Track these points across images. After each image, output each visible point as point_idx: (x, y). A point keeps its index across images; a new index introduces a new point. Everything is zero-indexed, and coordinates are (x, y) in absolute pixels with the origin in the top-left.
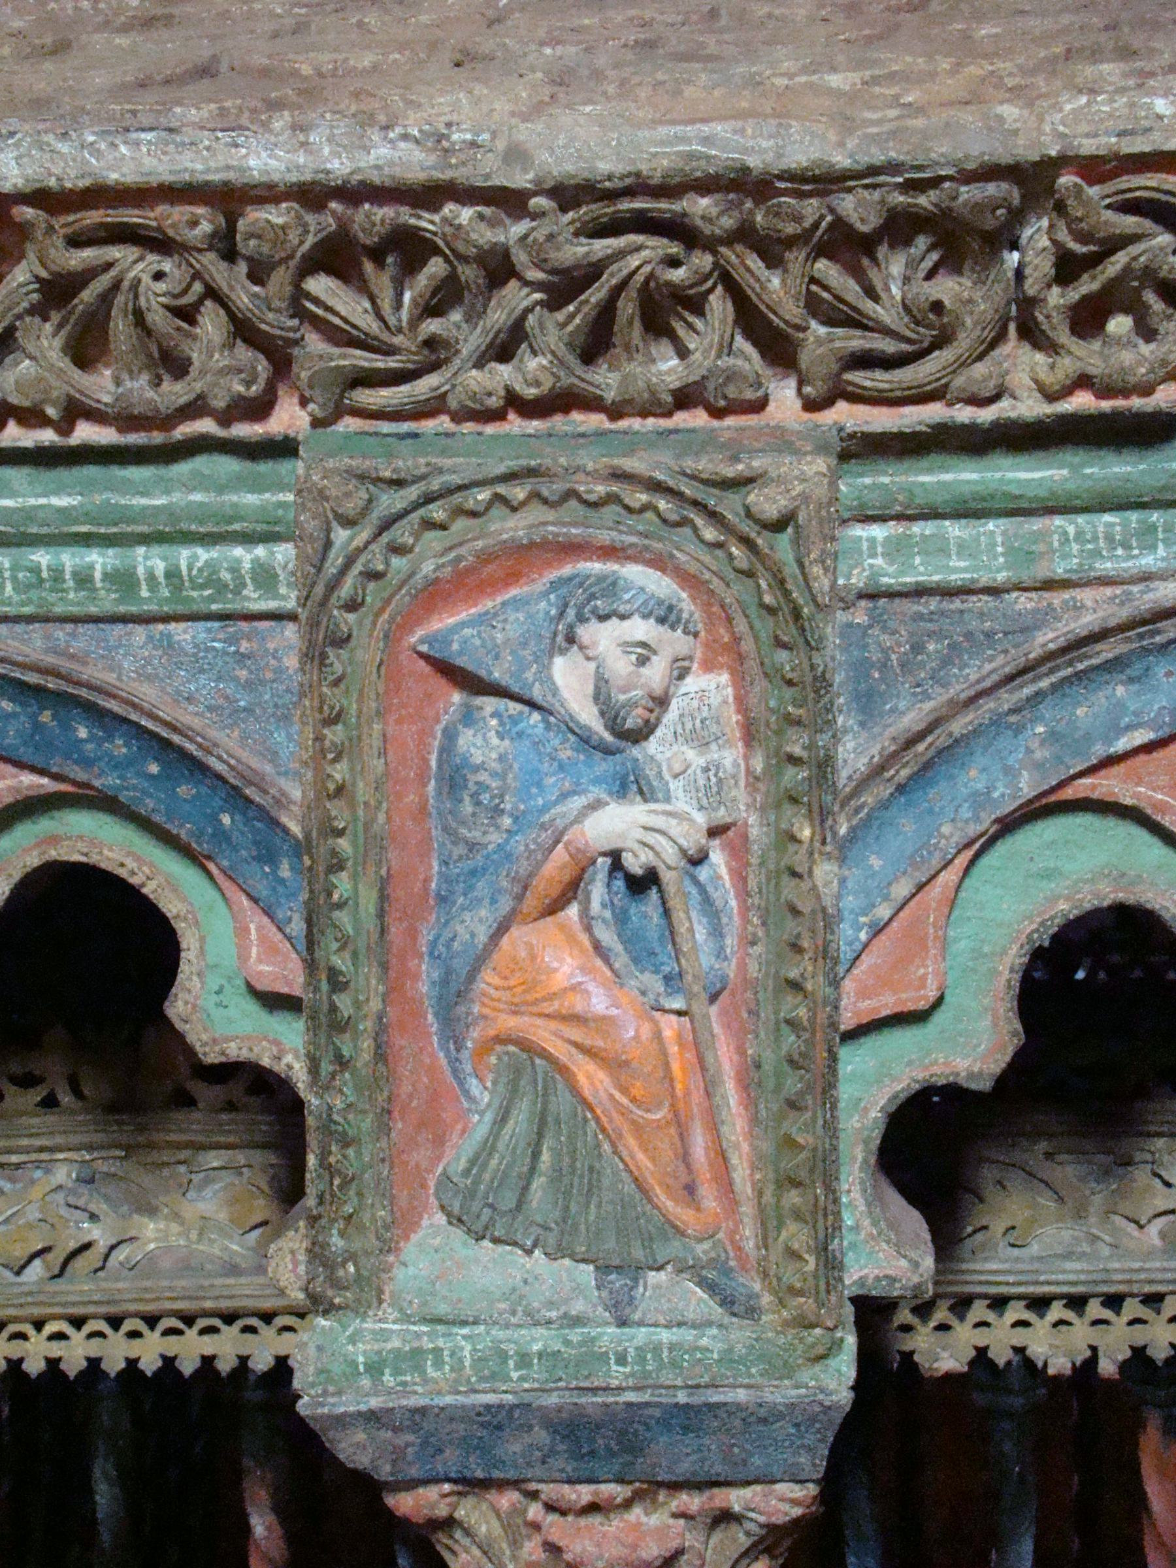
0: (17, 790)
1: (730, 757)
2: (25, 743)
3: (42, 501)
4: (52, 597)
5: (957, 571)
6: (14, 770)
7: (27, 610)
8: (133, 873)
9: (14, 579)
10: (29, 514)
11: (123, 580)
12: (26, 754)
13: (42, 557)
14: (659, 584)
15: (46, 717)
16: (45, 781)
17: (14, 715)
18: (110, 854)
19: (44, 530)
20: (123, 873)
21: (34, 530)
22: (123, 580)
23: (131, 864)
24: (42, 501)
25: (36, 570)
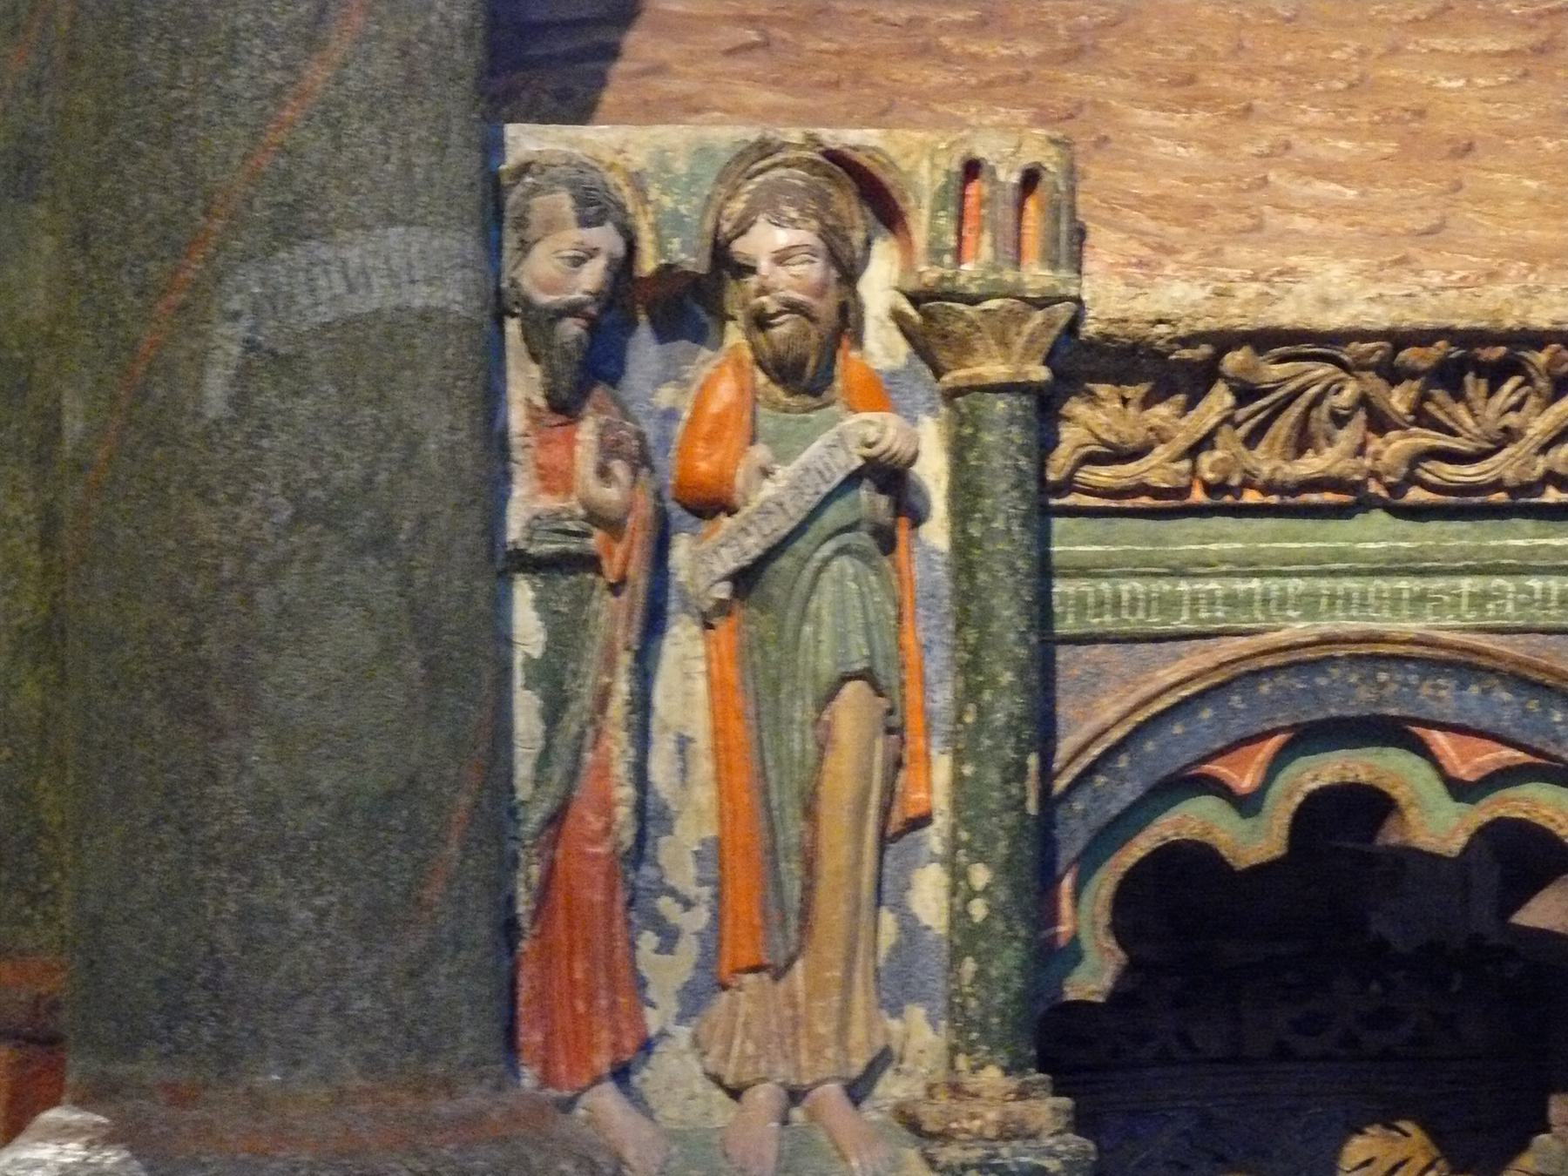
0: (1497, 761)
2: (1516, 726)
3: (1544, 541)
4: (1540, 613)
6: (1496, 746)
7: (1520, 623)
8: (1561, 827)
9: (1515, 600)
10: (1533, 550)
12: (1515, 733)
13: (1535, 583)
15: (1533, 705)
16: (1519, 754)
17: (1508, 704)
18: (1545, 812)
19: (1543, 563)
20: (1551, 826)
21: (1534, 563)
23: (1560, 819)
24: (1544, 541)
25: (1531, 592)
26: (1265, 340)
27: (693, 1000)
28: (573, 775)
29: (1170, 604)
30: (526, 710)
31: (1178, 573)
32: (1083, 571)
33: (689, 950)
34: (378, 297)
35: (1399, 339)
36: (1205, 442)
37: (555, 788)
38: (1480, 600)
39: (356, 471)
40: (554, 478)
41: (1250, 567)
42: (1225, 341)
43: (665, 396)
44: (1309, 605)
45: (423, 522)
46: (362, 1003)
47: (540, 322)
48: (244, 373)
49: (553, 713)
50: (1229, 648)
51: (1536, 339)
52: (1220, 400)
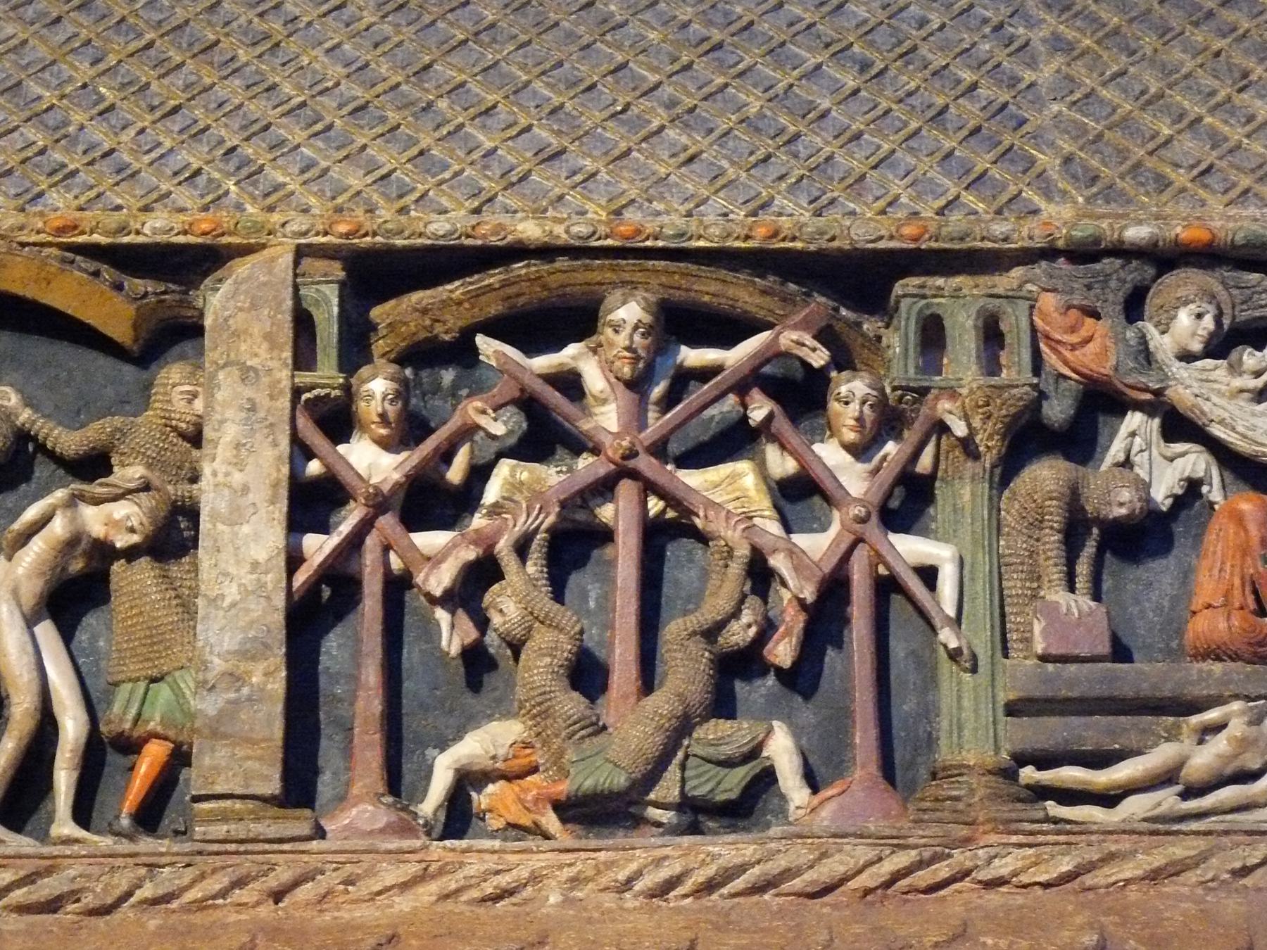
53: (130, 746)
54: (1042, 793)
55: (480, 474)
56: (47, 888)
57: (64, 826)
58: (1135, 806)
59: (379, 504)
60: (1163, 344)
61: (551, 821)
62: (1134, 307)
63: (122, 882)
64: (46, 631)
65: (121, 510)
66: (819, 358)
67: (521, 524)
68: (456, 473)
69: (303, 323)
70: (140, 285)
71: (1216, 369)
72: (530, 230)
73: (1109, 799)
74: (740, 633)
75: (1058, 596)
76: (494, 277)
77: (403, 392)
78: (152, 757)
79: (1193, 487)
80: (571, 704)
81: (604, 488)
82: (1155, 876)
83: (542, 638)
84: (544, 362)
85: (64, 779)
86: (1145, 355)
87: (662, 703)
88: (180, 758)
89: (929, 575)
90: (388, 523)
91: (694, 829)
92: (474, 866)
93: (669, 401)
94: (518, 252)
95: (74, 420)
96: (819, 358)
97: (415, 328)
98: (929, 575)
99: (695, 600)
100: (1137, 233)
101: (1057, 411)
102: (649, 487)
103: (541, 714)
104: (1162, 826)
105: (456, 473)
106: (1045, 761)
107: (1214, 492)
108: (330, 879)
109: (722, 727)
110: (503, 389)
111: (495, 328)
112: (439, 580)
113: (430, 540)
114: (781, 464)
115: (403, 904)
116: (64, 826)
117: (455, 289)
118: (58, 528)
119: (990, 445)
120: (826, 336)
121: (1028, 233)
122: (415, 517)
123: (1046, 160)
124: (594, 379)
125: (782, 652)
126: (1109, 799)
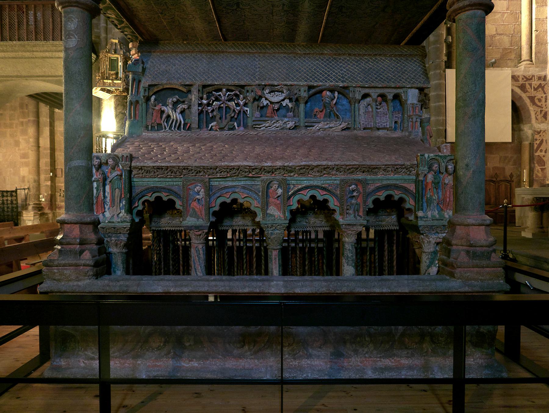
1: (203, 193)
5: (216, 184)
11: (173, 184)
14: (200, 185)
22: (173, 184)
26: (144, 166)
27: (109, 209)
28: (99, 194)
29: (143, 184)
30: (95, 191)
31: (143, 182)
32: (137, 182)
33: (108, 206)
34: (77, 164)
35: (154, 167)
36: (143, 173)
37: (97, 195)
38: (165, 184)
39: (75, 175)
40: (97, 176)
41: (148, 181)
42: (142, 167)
43: (107, 170)
44: (153, 184)
45: (81, 179)
46: (75, 208)
47: (95, 166)
48: (68, 169)
49: (97, 191)
50: (147, 187)
51: (164, 166)
52: (143, 171)
53: (187, 124)
54: (255, 127)
55: (213, 102)
56: (180, 135)
57: (182, 130)
58: (262, 129)
59: (205, 105)
60: (265, 92)
61: (218, 130)
62: (263, 89)
63: (186, 134)
64: (180, 114)
65: (186, 105)
66: (239, 93)
67: (216, 107)
68: (211, 102)
69: (199, 90)
70: (187, 87)
71: (269, 94)
72: (216, 83)
73: (260, 128)
74: (233, 115)
75: (257, 112)
76: (213, 87)
77: (207, 96)
78: (188, 125)
79: (268, 104)
80: (220, 121)
81: (222, 104)
82: (263, 134)
83: (217, 116)
84: (218, 94)
85: (182, 126)
86: (264, 94)
87: (227, 121)
88: (191, 124)
89: (247, 111)
90: (206, 106)
91: (229, 130)
92: (212, 133)
93: (228, 97)
94: (215, 85)
95: (182, 98)
96: (239, 93)
97: (208, 91)
98: (247, 111)
99: (229, 113)
100: (263, 84)
101: (257, 98)
102: (226, 104)
103: (218, 122)
104: (263, 130)
105: (211, 102)
106: (255, 125)
107: (269, 104)
108: (202, 134)
109: (231, 122)
110: (215, 96)
111: (214, 91)
112: (210, 111)
113: (209, 108)
114: (236, 102)
115: (207, 136)
116: (182, 130)
117: (211, 88)
118: (181, 107)
119: (252, 100)
120: (239, 92)
121: (255, 84)
122: (208, 106)
123: (257, 78)
124: (222, 95)
125: (236, 117)
126: (260, 128)
